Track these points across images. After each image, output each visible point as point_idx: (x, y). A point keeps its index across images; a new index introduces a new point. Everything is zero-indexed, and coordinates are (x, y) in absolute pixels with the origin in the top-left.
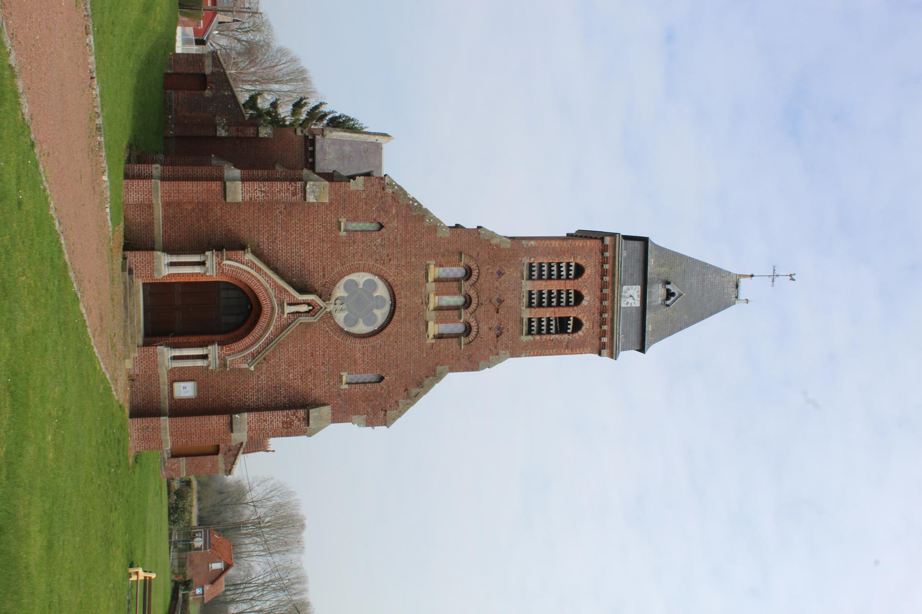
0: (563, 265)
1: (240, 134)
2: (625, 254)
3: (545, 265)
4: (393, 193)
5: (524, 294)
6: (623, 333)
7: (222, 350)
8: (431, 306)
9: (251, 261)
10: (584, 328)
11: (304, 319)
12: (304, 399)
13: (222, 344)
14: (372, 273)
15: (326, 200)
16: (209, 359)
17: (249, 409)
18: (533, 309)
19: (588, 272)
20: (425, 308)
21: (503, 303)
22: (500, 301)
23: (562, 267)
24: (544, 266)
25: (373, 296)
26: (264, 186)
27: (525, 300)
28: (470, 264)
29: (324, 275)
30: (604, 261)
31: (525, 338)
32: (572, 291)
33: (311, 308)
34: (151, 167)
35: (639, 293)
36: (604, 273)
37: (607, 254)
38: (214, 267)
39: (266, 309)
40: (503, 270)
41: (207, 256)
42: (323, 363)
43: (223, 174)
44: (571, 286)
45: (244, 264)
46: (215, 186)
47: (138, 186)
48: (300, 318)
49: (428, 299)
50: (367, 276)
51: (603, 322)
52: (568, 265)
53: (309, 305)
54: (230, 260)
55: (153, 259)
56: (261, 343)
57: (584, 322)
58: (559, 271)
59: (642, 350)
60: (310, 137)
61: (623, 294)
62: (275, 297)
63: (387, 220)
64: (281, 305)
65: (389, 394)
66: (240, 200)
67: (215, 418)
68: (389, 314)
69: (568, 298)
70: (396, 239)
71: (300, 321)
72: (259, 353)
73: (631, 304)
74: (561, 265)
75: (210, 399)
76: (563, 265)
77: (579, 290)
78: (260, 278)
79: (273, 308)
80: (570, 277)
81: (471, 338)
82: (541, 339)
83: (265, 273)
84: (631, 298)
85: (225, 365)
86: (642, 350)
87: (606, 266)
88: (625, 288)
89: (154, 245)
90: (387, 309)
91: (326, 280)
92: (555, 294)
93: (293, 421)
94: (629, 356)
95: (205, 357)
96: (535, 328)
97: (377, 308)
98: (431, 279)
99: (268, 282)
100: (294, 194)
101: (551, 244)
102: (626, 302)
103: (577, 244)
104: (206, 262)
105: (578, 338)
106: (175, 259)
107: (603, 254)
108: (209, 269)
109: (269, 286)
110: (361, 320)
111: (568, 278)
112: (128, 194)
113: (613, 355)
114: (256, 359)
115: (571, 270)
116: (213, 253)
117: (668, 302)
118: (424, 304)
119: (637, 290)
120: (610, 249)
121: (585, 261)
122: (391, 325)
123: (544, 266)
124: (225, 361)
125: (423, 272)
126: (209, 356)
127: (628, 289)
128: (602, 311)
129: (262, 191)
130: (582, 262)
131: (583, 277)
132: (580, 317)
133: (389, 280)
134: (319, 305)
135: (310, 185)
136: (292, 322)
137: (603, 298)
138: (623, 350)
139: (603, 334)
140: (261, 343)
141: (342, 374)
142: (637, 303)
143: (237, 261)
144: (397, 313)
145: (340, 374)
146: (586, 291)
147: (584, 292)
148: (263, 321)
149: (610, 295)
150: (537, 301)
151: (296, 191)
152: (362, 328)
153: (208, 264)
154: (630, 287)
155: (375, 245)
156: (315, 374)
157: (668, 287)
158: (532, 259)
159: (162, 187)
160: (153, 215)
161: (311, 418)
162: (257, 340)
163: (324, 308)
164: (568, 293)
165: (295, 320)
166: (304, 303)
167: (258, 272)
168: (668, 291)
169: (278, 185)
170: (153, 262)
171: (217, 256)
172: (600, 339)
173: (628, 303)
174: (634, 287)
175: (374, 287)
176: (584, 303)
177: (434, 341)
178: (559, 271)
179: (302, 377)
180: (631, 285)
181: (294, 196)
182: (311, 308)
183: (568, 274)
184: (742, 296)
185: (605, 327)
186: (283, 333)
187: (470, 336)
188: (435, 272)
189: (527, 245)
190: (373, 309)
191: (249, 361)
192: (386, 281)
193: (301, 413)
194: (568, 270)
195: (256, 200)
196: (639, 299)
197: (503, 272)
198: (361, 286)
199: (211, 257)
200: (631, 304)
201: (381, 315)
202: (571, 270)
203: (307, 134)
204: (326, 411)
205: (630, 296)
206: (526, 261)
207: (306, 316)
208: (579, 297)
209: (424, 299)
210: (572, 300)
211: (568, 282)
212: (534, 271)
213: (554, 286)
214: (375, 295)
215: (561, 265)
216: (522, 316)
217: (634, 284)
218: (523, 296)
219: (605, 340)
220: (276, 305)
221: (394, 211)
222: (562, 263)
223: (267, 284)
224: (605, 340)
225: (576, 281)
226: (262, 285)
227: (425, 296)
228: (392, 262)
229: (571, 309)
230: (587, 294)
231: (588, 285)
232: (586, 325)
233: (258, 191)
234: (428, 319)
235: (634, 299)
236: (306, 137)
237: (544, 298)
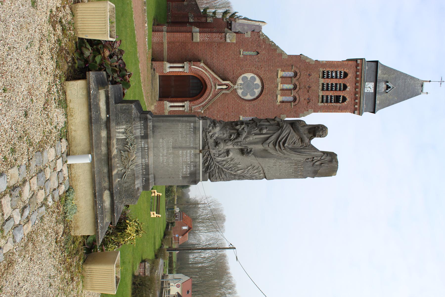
1: (199, 21)
2: (367, 68)
4: (263, 39)
5: (320, 85)
8: (279, 88)
10: (347, 101)
11: (224, 91)
13: (190, 101)
14: (254, 73)
15: (234, 41)
16: (185, 107)
18: (324, 91)
19: (349, 76)
20: (276, 89)
21: (311, 88)
22: (309, 87)
26: (209, 35)
27: (321, 87)
28: (297, 70)
29: (233, 74)
30: (357, 71)
31: (320, 104)
33: (228, 87)
36: (357, 76)
37: (359, 68)
39: (209, 87)
42: (232, 111)
43: (192, 30)
44: (341, 81)
46: (189, 35)
49: (278, 85)
50: (252, 75)
51: (356, 98)
52: (341, 72)
53: (227, 85)
57: (347, 98)
58: (336, 75)
59: (374, 112)
60: (230, 22)
61: (366, 86)
64: (215, 86)
69: (340, 87)
70: (264, 59)
72: (205, 105)
74: (337, 72)
77: (345, 83)
78: (206, 73)
79: (212, 87)
81: (296, 103)
82: (327, 105)
83: (209, 71)
84: (369, 88)
85: (191, 110)
87: (358, 73)
88: (367, 83)
90: (260, 89)
92: (334, 85)
94: (367, 115)
95: (183, 106)
96: (326, 100)
97: (256, 89)
98: (279, 77)
102: (367, 90)
103: (345, 63)
105: (344, 105)
106: (172, 65)
107: (356, 68)
109: (210, 77)
110: (249, 94)
111: (340, 78)
113: (360, 114)
115: (342, 75)
117: (387, 91)
119: (372, 85)
120: (360, 65)
121: (348, 70)
122: (261, 96)
125: (276, 73)
127: (368, 84)
128: (356, 93)
129: (208, 37)
130: (347, 71)
131: (347, 78)
132: (345, 96)
134: (231, 86)
137: (356, 87)
138: (365, 112)
139: (356, 104)
141: (240, 116)
142: (372, 91)
146: (349, 84)
147: (348, 85)
148: (207, 92)
149: (360, 86)
152: (249, 97)
153: (185, 67)
154: (369, 83)
155: (255, 61)
157: (388, 84)
158: (324, 69)
160: (163, 47)
164: (340, 85)
165: (221, 92)
168: (387, 86)
170: (163, 66)
171: (189, 64)
172: (354, 106)
173: (368, 90)
175: (255, 79)
176: (348, 89)
177: (280, 104)
180: (369, 82)
182: (228, 87)
183: (340, 76)
184: (425, 91)
190: (254, 89)
194: (340, 75)
196: (373, 89)
198: (249, 79)
199: (186, 65)
201: (257, 91)
202: (342, 75)
203: (228, 21)
205: (369, 87)
206: (321, 70)
208: (345, 87)
209: (276, 85)
211: (340, 80)
212: (325, 74)
213: (334, 81)
215: (337, 72)
216: (319, 94)
219: (356, 106)
221: (264, 47)
222: (338, 71)
224: (356, 106)
225: (344, 79)
226: (207, 76)
227: (277, 84)
228: (262, 69)
229: (341, 92)
231: (349, 82)
232: (348, 100)
233: (206, 37)
234: (277, 94)
235: (371, 89)
236: (228, 22)
237: (329, 87)
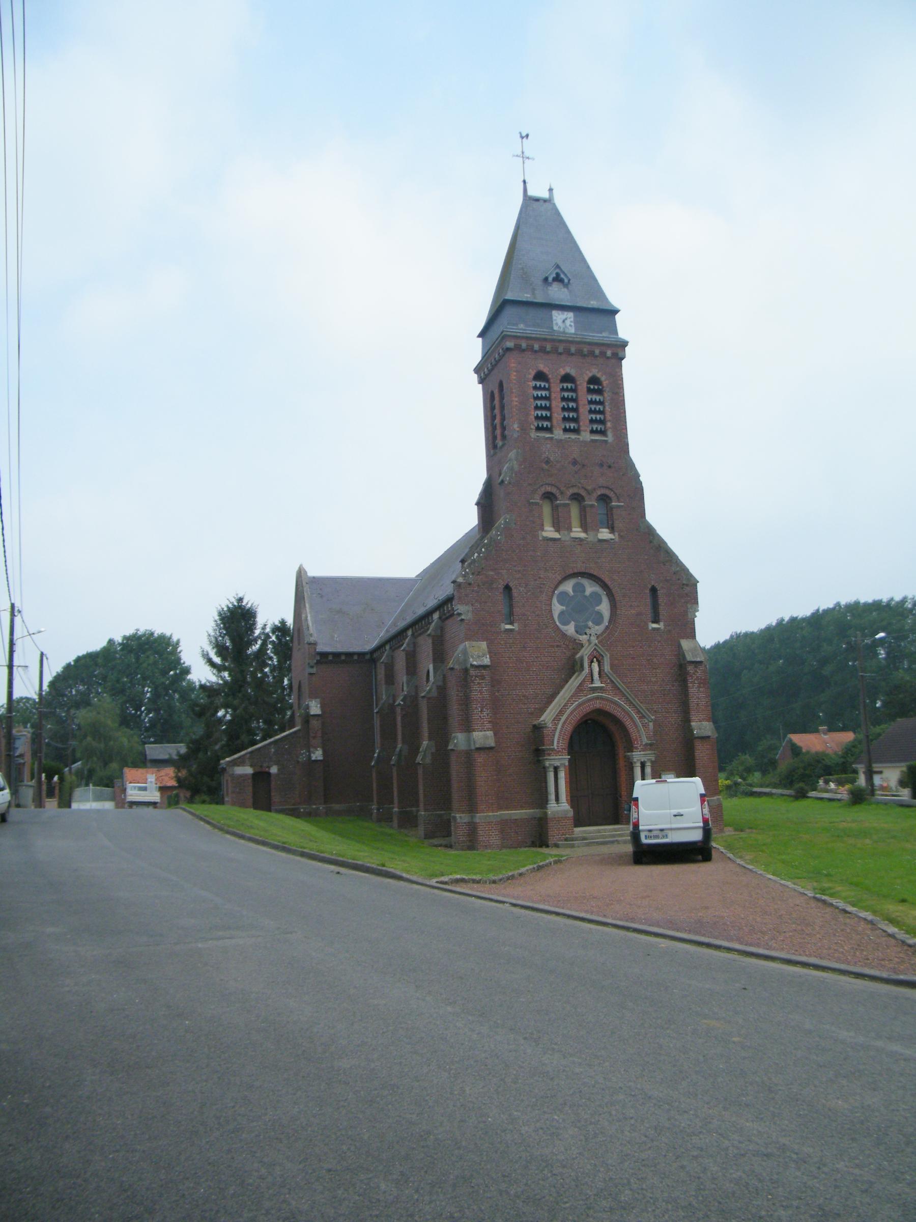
0: (535, 393)
1: (319, 734)
2: (522, 326)
3: (536, 412)
4: (473, 574)
5: (568, 436)
6: (601, 333)
7: (637, 748)
8: (583, 535)
9: (553, 720)
10: (598, 375)
11: (607, 668)
12: (674, 666)
13: (630, 747)
14: (552, 596)
15: (484, 645)
16: (646, 760)
17: (687, 720)
18: (582, 428)
19: (542, 367)
20: (585, 542)
21: (578, 459)
22: (575, 462)
23: (537, 395)
24: (537, 414)
25: (573, 596)
26: (476, 708)
27: (573, 436)
28: (541, 493)
29: (558, 646)
30: (530, 349)
31: (610, 438)
32: (561, 385)
33: (595, 659)
34: (459, 823)
35: (560, 312)
36: (543, 350)
37: (524, 345)
38: (561, 757)
39: (598, 705)
40: (544, 459)
41: (550, 765)
42: (641, 647)
43: (463, 751)
44: (556, 387)
45: (556, 728)
46: (480, 759)
47: (484, 835)
48: (606, 670)
49: (576, 538)
50: (555, 601)
51: (591, 354)
52: (535, 388)
53: (592, 662)
54: (553, 742)
55: (555, 818)
56: (630, 709)
57: (590, 375)
58: (542, 398)
59: (615, 312)
60: (318, 658)
61: (561, 330)
62: (586, 696)
63: (501, 581)
64: (594, 690)
65: (667, 581)
66: (491, 732)
67: (698, 754)
68: (591, 579)
69: (567, 390)
70: (519, 571)
71: (609, 670)
72: (639, 711)
73: (571, 322)
74: (535, 396)
75: (676, 759)
76: (535, 393)
77: (560, 377)
78: (568, 711)
79: (597, 698)
80: (547, 386)
81: (611, 495)
82: (610, 421)
83: (564, 706)
84: (566, 321)
85: (651, 745)
86: (615, 312)
87: (536, 347)
88: (555, 328)
89: (535, 818)
90: (585, 582)
91: (562, 643)
92: (564, 403)
93: (697, 677)
94: (624, 327)
95: (643, 766)
96: (599, 426)
97: (584, 591)
98: (557, 535)
99: (572, 704)
100: (483, 677)
101: (516, 405)
102: (570, 328)
103: (514, 378)
104: (555, 765)
105: (607, 382)
106: (552, 797)
108: (563, 762)
109: (577, 703)
110: (597, 608)
111: (548, 389)
112: (492, 845)
113: (624, 344)
114: (645, 715)
115: (540, 385)
116: (546, 759)
117: (566, 281)
118: (581, 543)
119: (556, 315)
121: (530, 370)
122: (602, 577)
123: (537, 414)
124: (646, 745)
125: (551, 543)
126: (642, 760)
127: (557, 324)
128: (580, 353)
129: (482, 711)
130: (533, 373)
131: (547, 373)
132: (586, 378)
133: (560, 579)
134: (592, 652)
135: (473, 661)
136: (609, 678)
137: (568, 352)
138: (616, 333)
139: (603, 354)
140: (630, 709)
141: (650, 628)
142: (570, 315)
143: (554, 735)
144: (592, 572)
145: (651, 630)
146: (561, 370)
147: (562, 372)
148: (608, 708)
149: (564, 345)
150: (572, 425)
151: (480, 676)
152: (604, 608)
153: (557, 763)
154: (554, 322)
155: (526, 593)
156: (651, 655)
157: (550, 279)
158: (532, 427)
159: (483, 811)
160: (507, 820)
161: (695, 660)
162: (627, 713)
163: (596, 647)
164: (563, 390)
165: (608, 676)
166: (590, 666)
167: (564, 714)
168: (555, 280)
169: (475, 695)
170: (558, 818)
171: (549, 755)
172: (608, 358)
173: (571, 326)
174: (554, 318)
175: (564, 594)
176: (573, 372)
177: (617, 534)
178: (542, 398)
179: (654, 668)
180: (552, 321)
181: (485, 678)
182: (595, 659)
183: (544, 389)
184: (545, 195)
185: (597, 352)
186: (620, 687)
187: (610, 495)
188: (549, 532)
189: (518, 431)
190: (586, 597)
191: (646, 721)
192: (560, 583)
193: (690, 669)
194: (540, 388)
195: (491, 716)
196: (566, 313)
197: (546, 459)
198: (564, 608)
199: (551, 761)
200: (571, 322)
201: (590, 588)
202: (540, 385)
203: (315, 661)
204: (685, 644)
205: (563, 322)
206: (534, 434)
207: (603, 665)
208: (567, 378)
209: (576, 543)
210: (569, 385)
211: (552, 390)
212: (543, 425)
213: (557, 404)
214: (572, 593)
215: (535, 396)
216: (589, 440)
217: (551, 318)
218: (569, 438)
219: (609, 353)
220: (594, 695)
221: (491, 573)
222: (534, 396)
223: (574, 704)
224: (609, 353)
225: (551, 381)
226: (575, 710)
227: (575, 541)
228: (542, 576)
229: (579, 387)
230: (564, 370)
231: (557, 368)
232: (595, 372)
233: (481, 714)
234: (596, 540)
235: (566, 319)
236: (318, 662)
237: (569, 416)
